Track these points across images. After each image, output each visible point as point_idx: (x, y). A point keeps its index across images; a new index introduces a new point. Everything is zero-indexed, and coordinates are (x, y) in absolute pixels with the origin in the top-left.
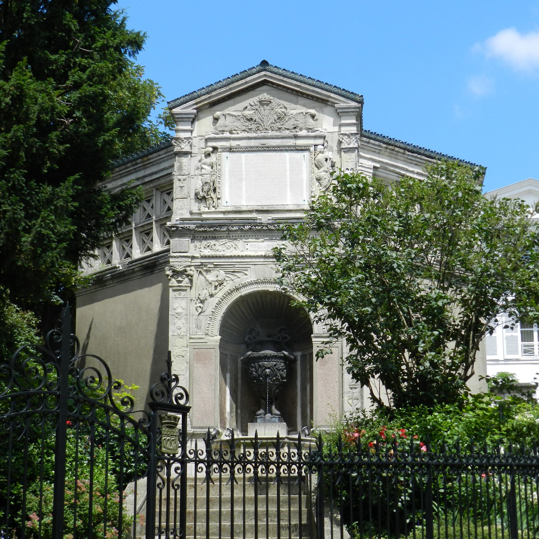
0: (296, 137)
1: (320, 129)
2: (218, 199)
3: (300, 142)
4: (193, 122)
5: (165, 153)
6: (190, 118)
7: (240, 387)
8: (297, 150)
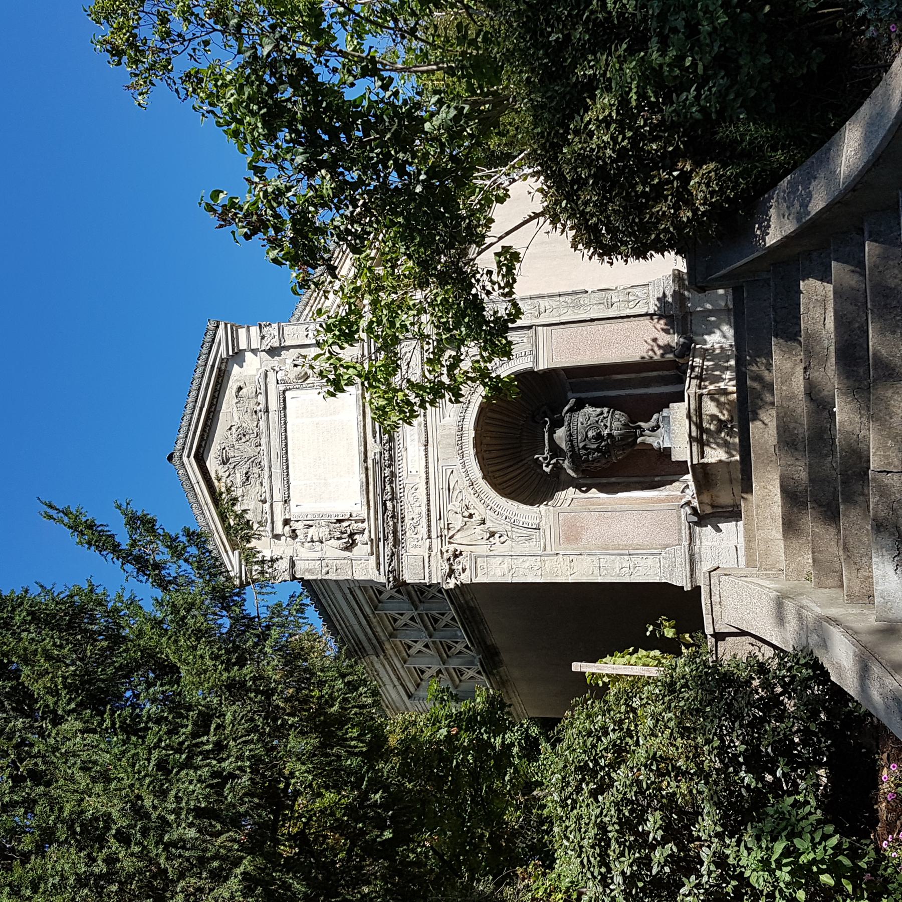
0: (267, 411)
1: (257, 377)
2: (351, 516)
3: (273, 405)
5: (325, 597)
8: (285, 408)
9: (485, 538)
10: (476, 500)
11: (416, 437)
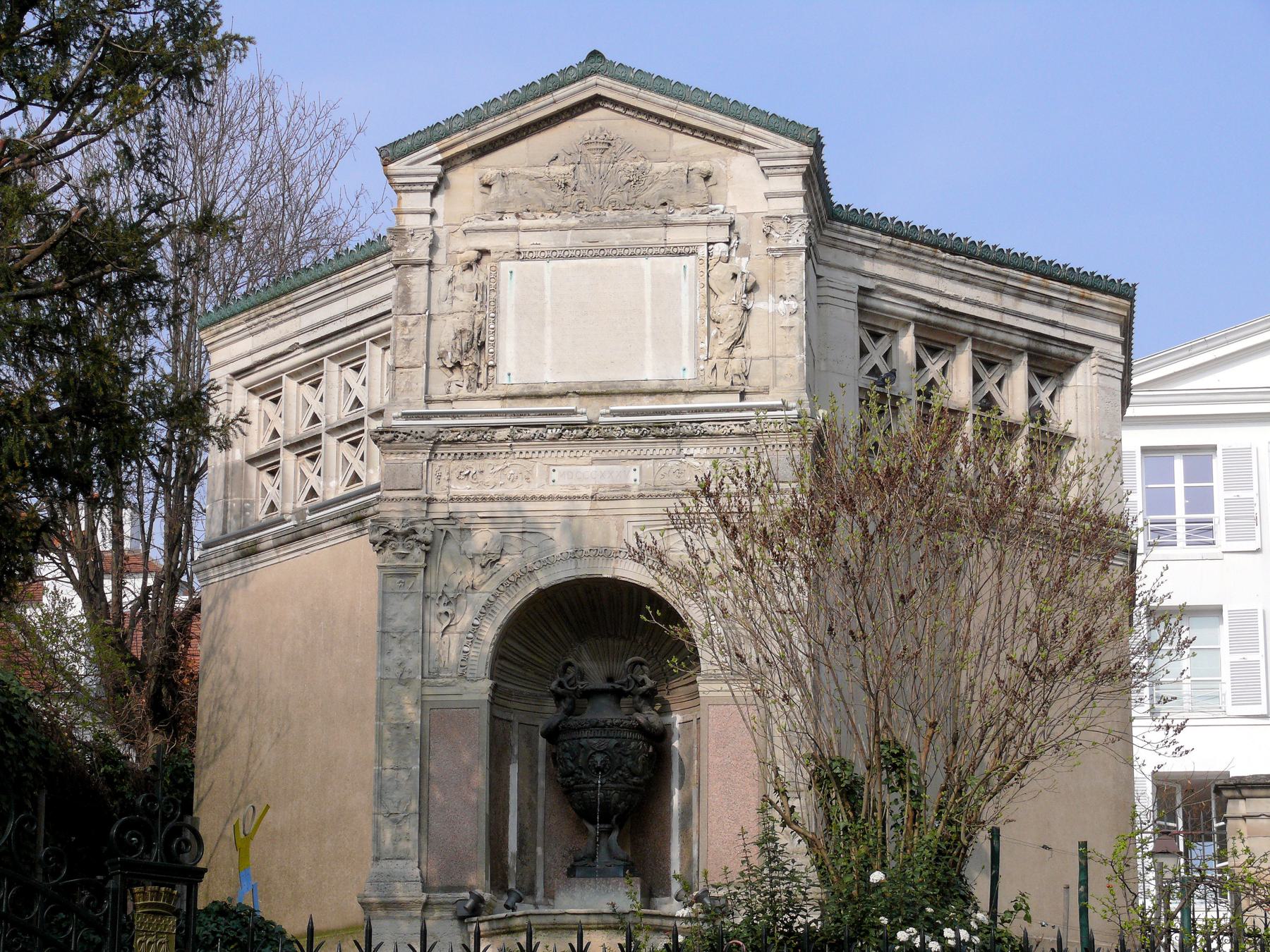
3: (676, 236)
4: (434, 194)
6: (428, 184)
7: (541, 794)
9: (446, 590)
10: (507, 575)
11: (606, 482)
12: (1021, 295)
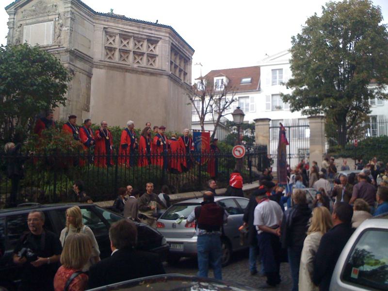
3: (50, 17)
4: (15, 14)
12: (144, 28)
